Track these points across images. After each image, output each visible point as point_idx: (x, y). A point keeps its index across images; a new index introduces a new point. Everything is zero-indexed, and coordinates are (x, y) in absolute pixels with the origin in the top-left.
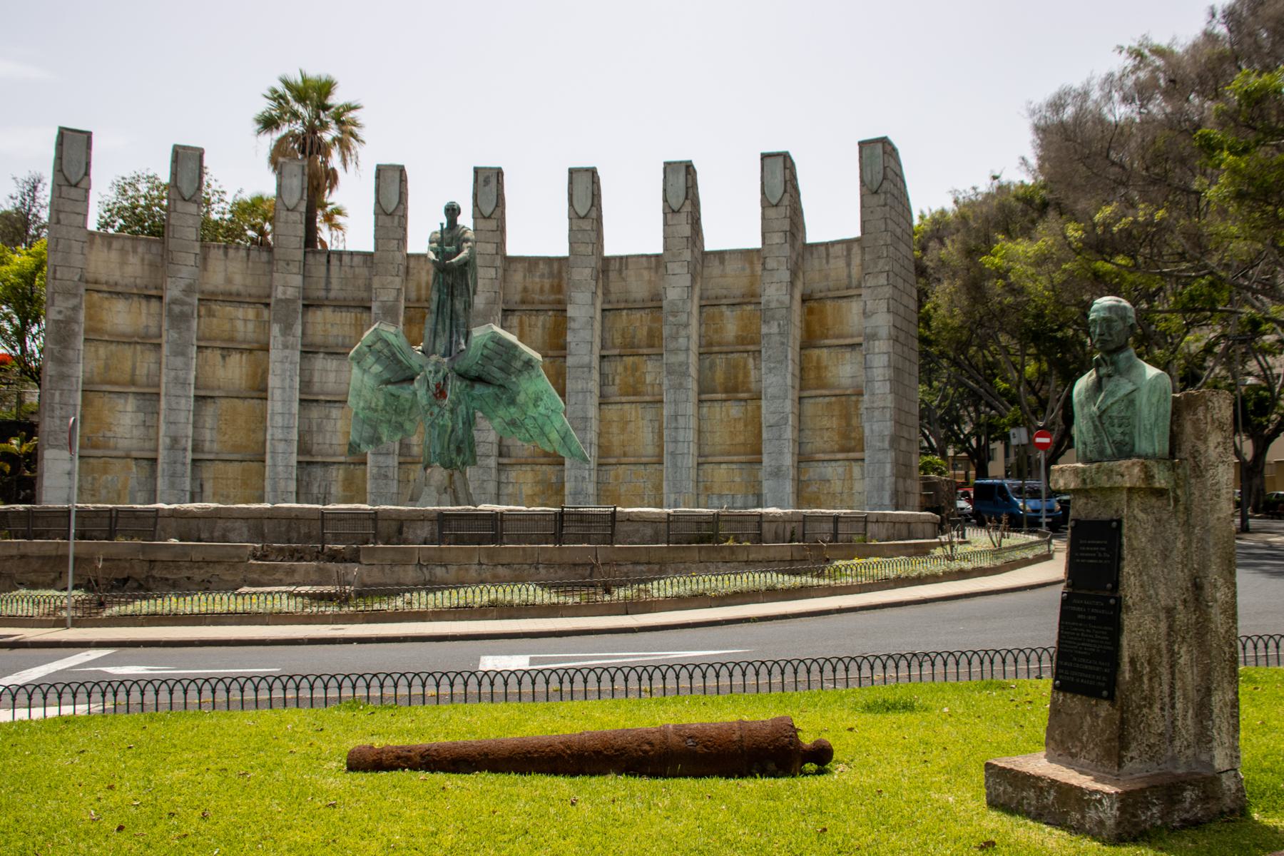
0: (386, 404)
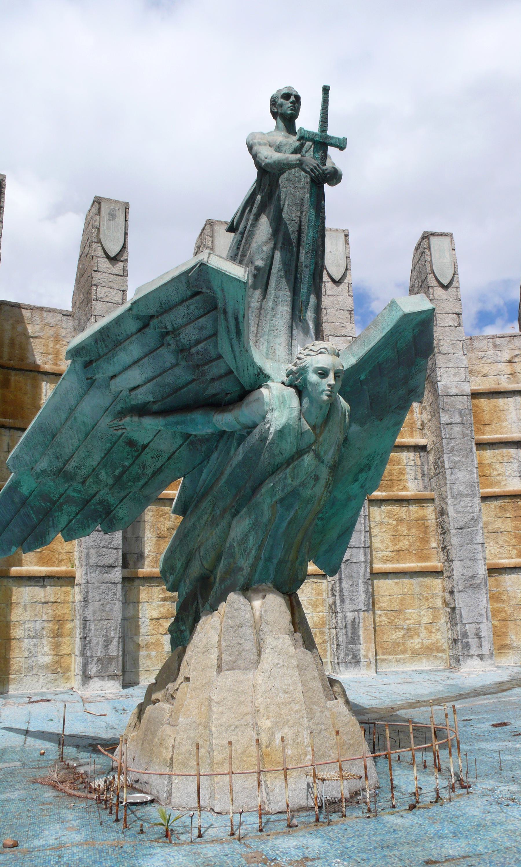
0: (104, 462)
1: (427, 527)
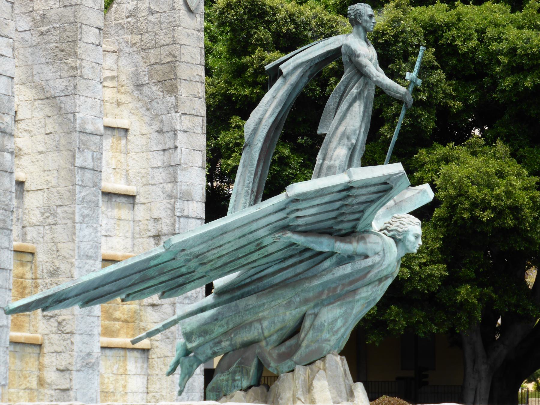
1: (24, 288)
